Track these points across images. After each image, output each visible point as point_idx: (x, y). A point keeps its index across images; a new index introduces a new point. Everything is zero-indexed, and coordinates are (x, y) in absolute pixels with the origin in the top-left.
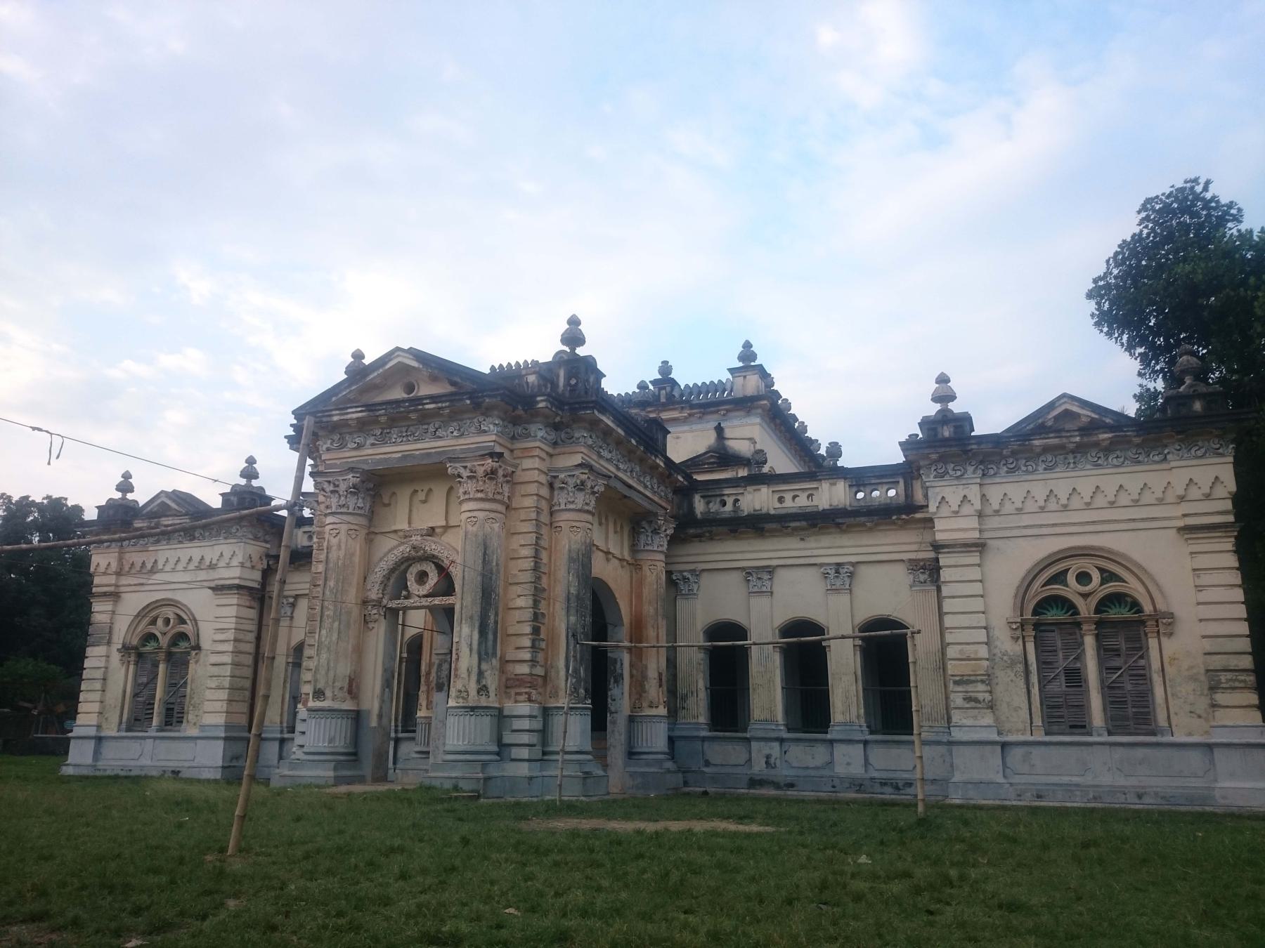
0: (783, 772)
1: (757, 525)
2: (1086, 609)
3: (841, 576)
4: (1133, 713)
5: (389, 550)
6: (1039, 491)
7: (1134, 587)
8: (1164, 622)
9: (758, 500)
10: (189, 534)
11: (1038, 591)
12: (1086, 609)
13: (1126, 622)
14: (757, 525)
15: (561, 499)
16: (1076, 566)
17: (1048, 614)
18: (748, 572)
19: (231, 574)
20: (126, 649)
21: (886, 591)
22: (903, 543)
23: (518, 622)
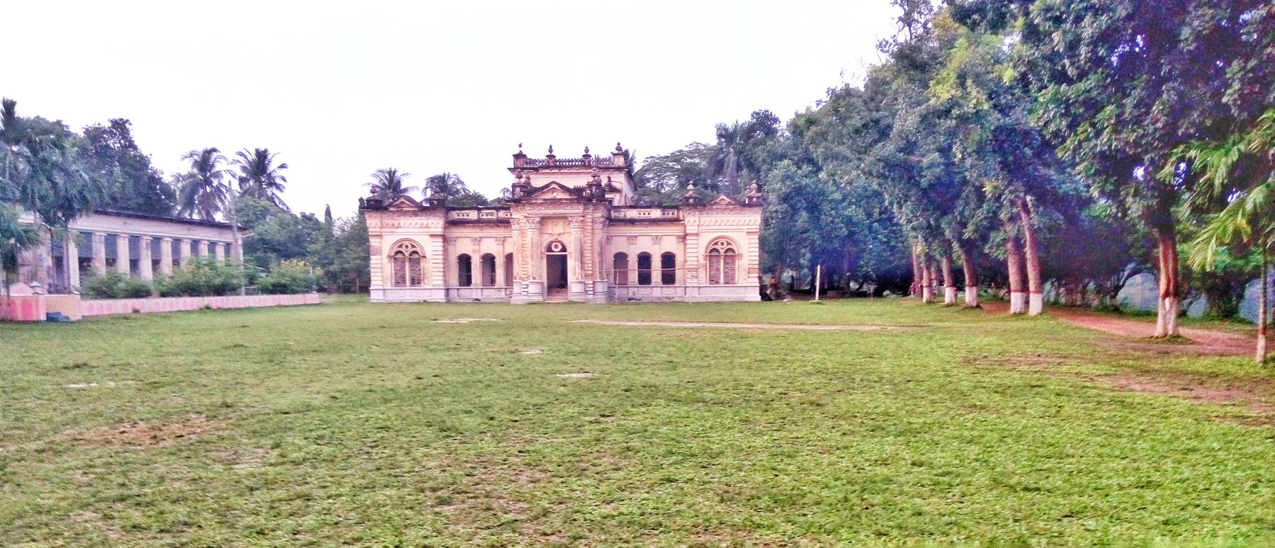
0: (638, 296)
1: (632, 222)
2: (722, 252)
3: (657, 239)
4: (730, 280)
5: (547, 239)
6: (714, 219)
7: (734, 247)
8: (740, 255)
9: (633, 214)
10: (415, 214)
11: (711, 247)
12: (722, 252)
13: (731, 255)
14: (632, 222)
15: (596, 226)
16: (721, 241)
17: (712, 253)
18: (629, 238)
19: (439, 230)
20: (389, 256)
21: (670, 245)
22: (676, 230)
23: (588, 259)
